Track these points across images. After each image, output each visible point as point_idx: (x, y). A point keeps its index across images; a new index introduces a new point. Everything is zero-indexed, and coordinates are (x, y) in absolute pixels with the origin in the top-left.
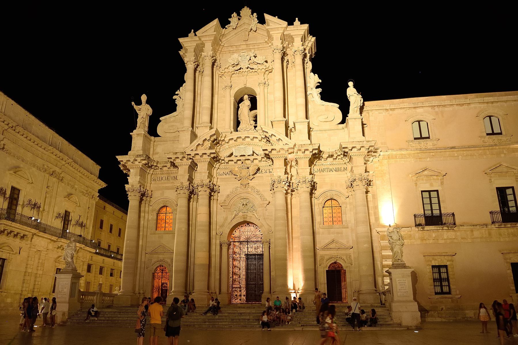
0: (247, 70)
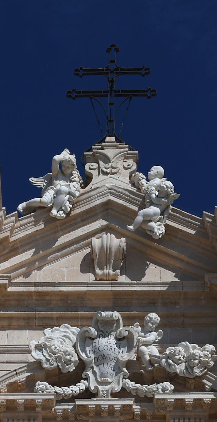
0: (118, 403)
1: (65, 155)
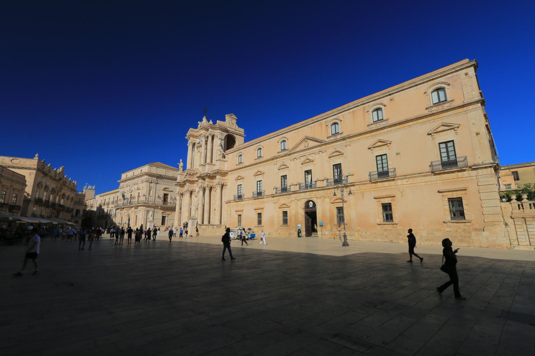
1: (199, 122)
